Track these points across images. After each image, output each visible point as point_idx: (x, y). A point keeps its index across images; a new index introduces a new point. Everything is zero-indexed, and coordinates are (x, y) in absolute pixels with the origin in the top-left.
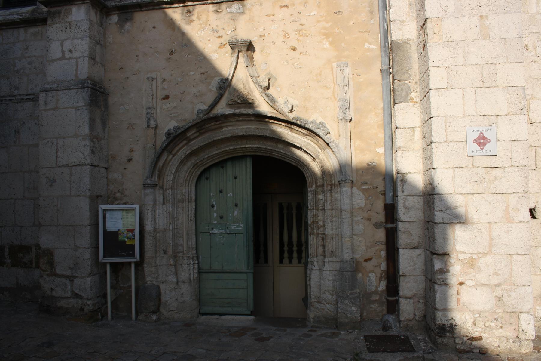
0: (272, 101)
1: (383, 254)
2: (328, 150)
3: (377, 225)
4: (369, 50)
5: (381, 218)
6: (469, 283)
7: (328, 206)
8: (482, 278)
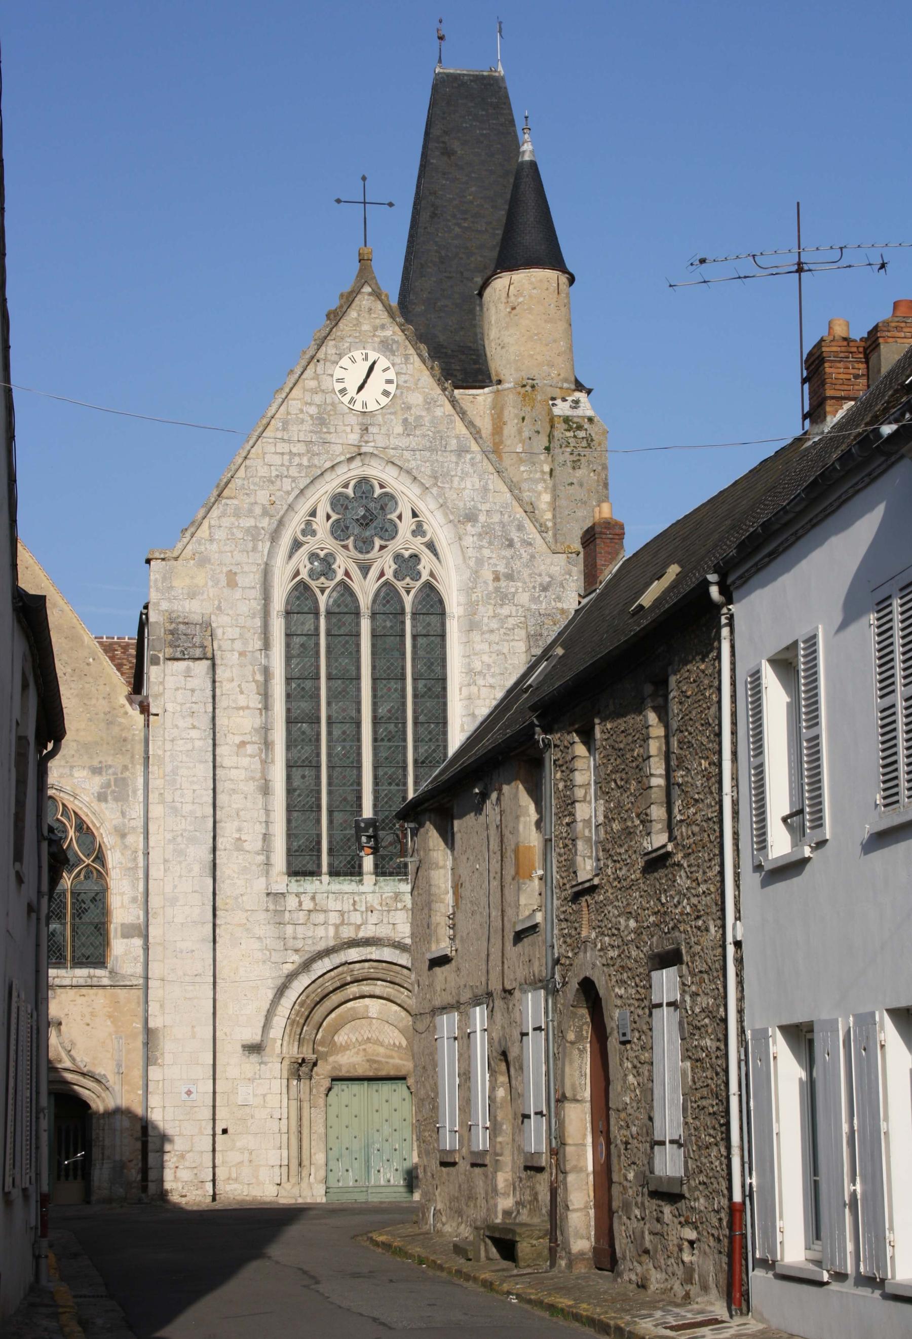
0: (73, 1059)
1: (140, 1157)
2: (107, 1092)
3: (137, 1139)
4: (135, 1028)
5: (139, 1134)
6: (181, 1167)
7: (106, 1127)
8: (187, 1164)
